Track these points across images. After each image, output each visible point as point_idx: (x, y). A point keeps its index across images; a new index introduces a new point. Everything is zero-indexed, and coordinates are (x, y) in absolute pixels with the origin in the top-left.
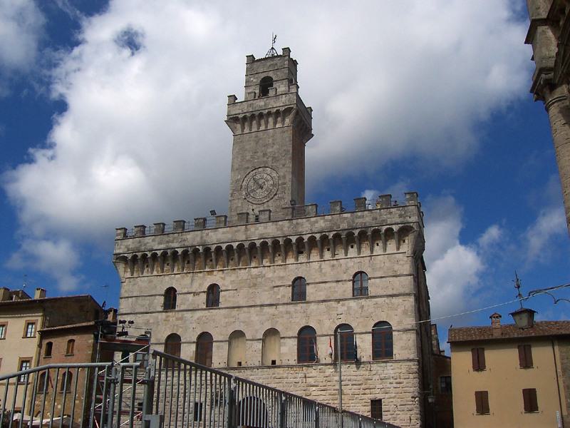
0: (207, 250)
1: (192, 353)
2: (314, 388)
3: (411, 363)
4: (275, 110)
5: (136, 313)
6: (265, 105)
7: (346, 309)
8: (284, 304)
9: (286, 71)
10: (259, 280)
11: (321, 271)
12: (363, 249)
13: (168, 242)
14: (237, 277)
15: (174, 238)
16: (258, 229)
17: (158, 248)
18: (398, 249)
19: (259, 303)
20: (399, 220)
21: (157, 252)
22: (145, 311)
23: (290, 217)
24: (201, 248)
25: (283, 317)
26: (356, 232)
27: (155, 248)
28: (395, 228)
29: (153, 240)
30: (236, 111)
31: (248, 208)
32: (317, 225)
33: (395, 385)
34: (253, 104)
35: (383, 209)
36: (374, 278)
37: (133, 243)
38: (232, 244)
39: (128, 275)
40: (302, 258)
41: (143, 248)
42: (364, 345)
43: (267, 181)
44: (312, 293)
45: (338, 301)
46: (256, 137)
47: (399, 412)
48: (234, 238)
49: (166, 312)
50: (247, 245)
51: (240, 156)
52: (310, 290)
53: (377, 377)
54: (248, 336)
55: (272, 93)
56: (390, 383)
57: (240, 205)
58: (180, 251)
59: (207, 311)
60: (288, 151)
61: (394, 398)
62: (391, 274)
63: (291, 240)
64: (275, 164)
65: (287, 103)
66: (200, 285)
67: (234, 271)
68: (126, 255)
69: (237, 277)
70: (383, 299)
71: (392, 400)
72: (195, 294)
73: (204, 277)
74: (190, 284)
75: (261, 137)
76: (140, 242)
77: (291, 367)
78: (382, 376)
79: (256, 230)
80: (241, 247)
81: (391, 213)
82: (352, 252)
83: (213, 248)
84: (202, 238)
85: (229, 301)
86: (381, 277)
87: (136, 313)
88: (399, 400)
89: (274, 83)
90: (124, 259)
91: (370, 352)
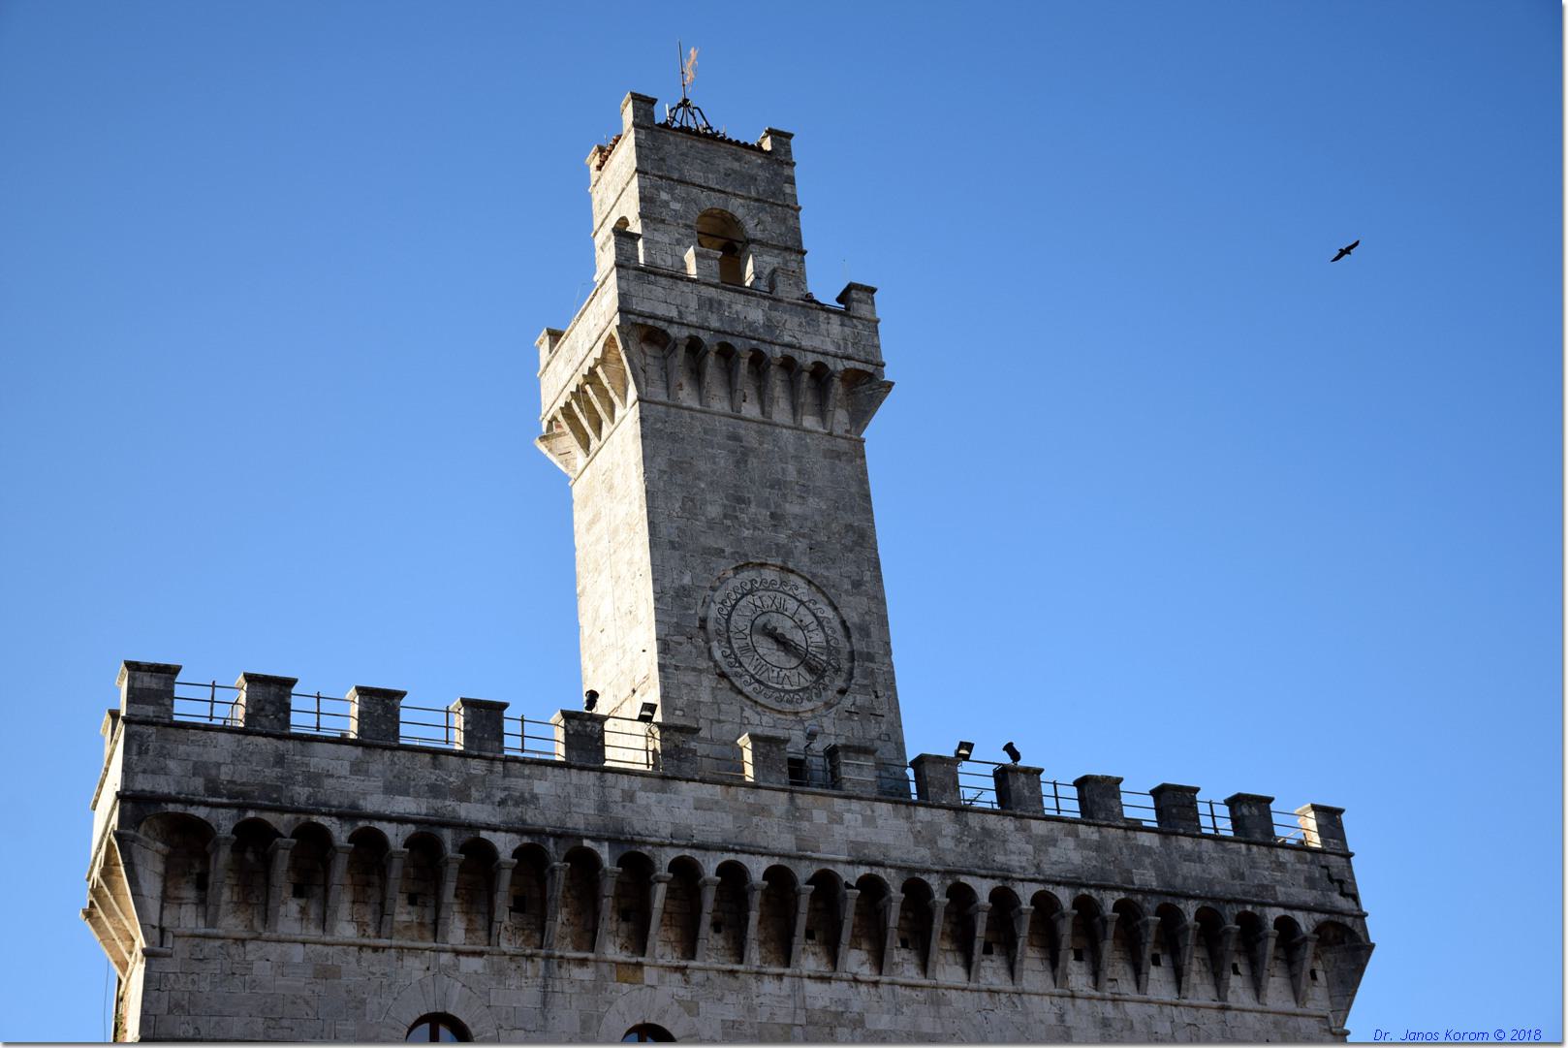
0: (636, 866)
6: (770, 326)
12: (1194, 978)
13: (435, 791)
14: (751, 1009)
15: (469, 780)
16: (836, 819)
17: (387, 810)
20: (1309, 897)
24: (604, 852)
26: (1190, 909)
30: (657, 302)
34: (720, 303)
38: (743, 859)
40: (992, 972)
41: (301, 793)
43: (801, 627)
48: (746, 838)
50: (804, 872)
57: (705, 696)
58: (505, 845)
64: (820, 570)
65: (850, 351)
67: (731, 980)
68: (201, 812)
73: (598, 987)
79: (831, 821)
80: (779, 877)
81: (1281, 866)
82: (1159, 980)
83: (665, 858)
84: (603, 807)
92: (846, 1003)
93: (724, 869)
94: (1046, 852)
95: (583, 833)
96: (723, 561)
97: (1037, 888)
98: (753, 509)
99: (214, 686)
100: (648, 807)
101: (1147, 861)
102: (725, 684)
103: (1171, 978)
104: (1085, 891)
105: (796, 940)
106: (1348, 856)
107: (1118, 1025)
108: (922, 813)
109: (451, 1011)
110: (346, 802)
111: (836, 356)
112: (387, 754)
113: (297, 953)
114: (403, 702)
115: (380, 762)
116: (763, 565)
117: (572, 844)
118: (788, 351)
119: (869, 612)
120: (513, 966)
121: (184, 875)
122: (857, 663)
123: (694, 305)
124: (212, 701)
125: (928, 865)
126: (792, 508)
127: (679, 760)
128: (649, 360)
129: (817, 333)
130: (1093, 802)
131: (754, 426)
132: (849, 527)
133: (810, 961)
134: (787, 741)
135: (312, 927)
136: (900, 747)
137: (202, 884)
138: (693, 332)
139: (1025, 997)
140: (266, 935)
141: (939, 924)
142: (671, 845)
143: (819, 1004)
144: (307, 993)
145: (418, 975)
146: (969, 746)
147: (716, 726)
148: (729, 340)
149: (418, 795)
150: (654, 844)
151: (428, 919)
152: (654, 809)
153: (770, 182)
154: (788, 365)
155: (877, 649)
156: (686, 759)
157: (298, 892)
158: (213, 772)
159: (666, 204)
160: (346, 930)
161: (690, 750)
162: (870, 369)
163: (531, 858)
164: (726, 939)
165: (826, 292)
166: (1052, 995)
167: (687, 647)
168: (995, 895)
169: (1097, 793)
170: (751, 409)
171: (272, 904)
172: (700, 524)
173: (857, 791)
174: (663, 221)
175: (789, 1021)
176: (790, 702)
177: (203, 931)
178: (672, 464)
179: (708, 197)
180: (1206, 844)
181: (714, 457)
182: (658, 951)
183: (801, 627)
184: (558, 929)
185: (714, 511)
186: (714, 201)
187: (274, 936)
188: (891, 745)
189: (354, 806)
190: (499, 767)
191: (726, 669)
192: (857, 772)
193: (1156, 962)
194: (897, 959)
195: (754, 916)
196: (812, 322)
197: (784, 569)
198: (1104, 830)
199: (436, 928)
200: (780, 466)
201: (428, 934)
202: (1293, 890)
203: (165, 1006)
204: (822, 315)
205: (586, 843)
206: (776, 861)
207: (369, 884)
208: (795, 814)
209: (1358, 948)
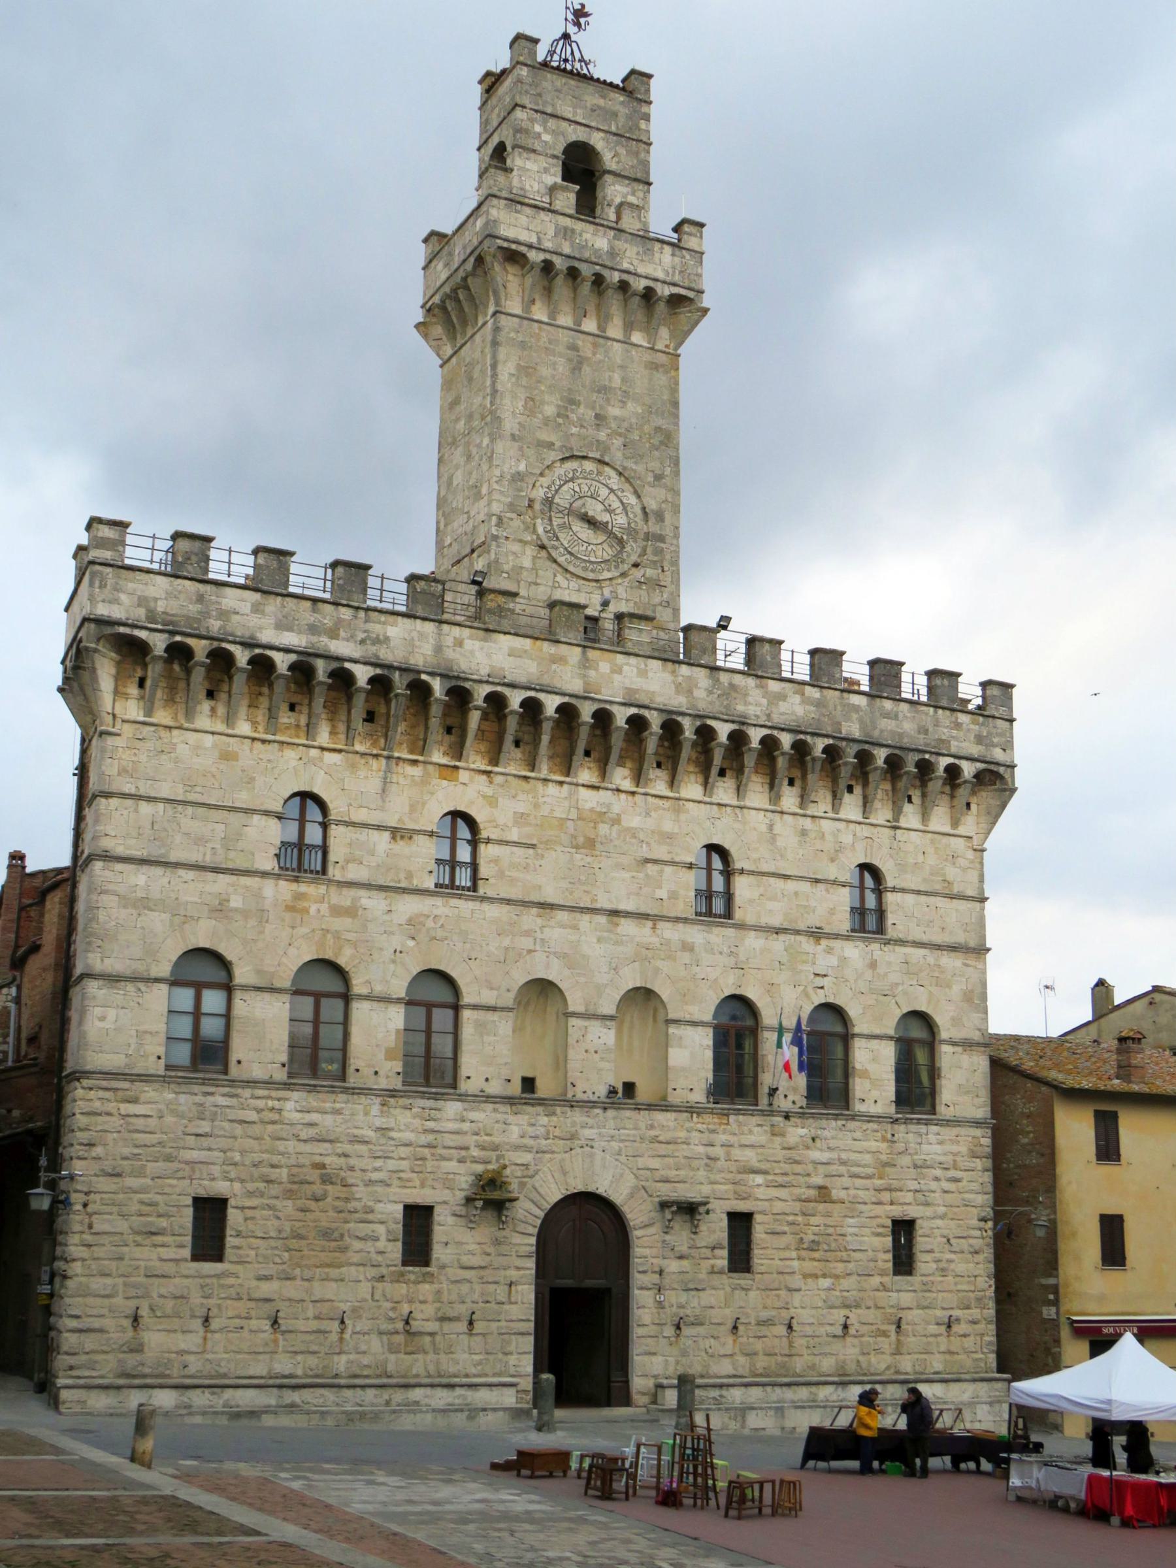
0: (459, 696)
1: (393, 1037)
2: (759, 1179)
3: (978, 1132)
5: (176, 865)
6: (612, 253)
7: (834, 961)
8: (677, 920)
10: (603, 829)
11: (773, 839)
12: (877, 804)
13: (313, 629)
14: (536, 806)
15: (339, 622)
16: (618, 670)
18: (955, 823)
19: (604, 903)
20: (975, 750)
22: (208, 860)
25: (675, 960)
26: (881, 755)
34: (573, 231)
35: (943, 708)
36: (903, 891)
37: (169, 595)
38: (541, 696)
39: (132, 709)
40: (724, 791)
42: (874, 1067)
43: (610, 511)
44: (751, 901)
45: (817, 934)
47: (953, 1256)
48: (546, 680)
49: (296, 880)
50: (586, 712)
51: (522, 395)
53: (905, 1160)
54: (575, 1003)
56: (937, 1179)
57: (527, 563)
59: (439, 901)
61: (942, 1217)
62: (938, 887)
64: (630, 464)
65: (677, 278)
66: (413, 808)
67: (523, 783)
68: (143, 634)
69: (536, 806)
70: (922, 952)
71: (939, 1222)
72: (397, 833)
73: (425, 781)
74: (386, 796)
75: (589, 354)
77: (691, 1110)
79: (613, 671)
80: (567, 712)
81: (958, 726)
82: (851, 806)
83: (481, 693)
85: (513, 881)
86: (919, 892)
87: (176, 865)
88: (952, 1223)
90: (131, 649)
91: (889, 1090)
92: (609, 806)
93: (525, 703)
94: (777, 705)
95: (421, 668)
96: (553, 453)
97: (766, 732)
98: (582, 410)
99: (154, 537)
100: (472, 652)
101: (855, 716)
102: (544, 553)
103: (861, 803)
104: (802, 737)
105: (575, 758)
106: (1011, 721)
107: (813, 835)
108: (684, 670)
109: (316, 791)
110: (247, 634)
111: (664, 282)
112: (279, 599)
113: (209, 740)
114: (293, 559)
115: (273, 605)
116: (584, 457)
117: (411, 677)
118: (625, 277)
119: (666, 501)
120: (363, 761)
121: (130, 677)
122: (651, 547)
123: (551, 233)
124: (153, 549)
125: (684, 709)
126: (614, 411)
127: (500, 616)
128: (510, 277)
129: (651, 261)
130: (820, 668)
131: (590, 338)
133: (586, 774)
134: (585, 607)
135: (219, 722)
136: (676, 612)
137: (141, 683)
138: (548, 256)
139: (745, 811)
140: (186, 725)
141: (686, 752)
142: (487, 682)
143: (588, 806)
144: (214, 769)
145: (294, 763)
146: (728, 619)
147: (533, 587)
148: (576, 264)
149: (300, 632)
150: (475, 681)
151: (303, 720)
152: (477, 654)
153: (629, 117)
154: (624, 286)
155: (668, 532)
156: (505, 617)
157: (210, 694)
158: (152, 604)
159: (539, 135)
160: (244, 728)
161: (509, 610)
162: (691, 294)
163: (381, 684)
164: (523, 753)
165: (661, 224)
166: (767, 811)
167: (517, 523)
168: (732, 736)
169: (825, 660)
170: (590, 325)
171: (191, 704)
172: (536, 421)
173: (636, 650)
174: (534, 151)
175: (564, 816)
176: (592, 571)
177: (141, 719)
178: (519, 367)
179: (575, 131)
180: (904, 707)
181: (555, 364)
182: (472, 758)
183: (610, 511)
184: (398, 737)
185: (550, 410)
186: (576, 134)
187: (191, 726)
188: (669, 611)
189: (252, 637)
190: (362, 614)
191: (546, 542)
193: (850, 789)
194: (651, 776)
195: (545, 739)
196: (649, 251)
197: (601, 462)
198: (826, 692)
199: (310, 730)
200: (607, 374)
201: (302, 734)
202: (964, 744)
203: (115, 771)
204: (657, 246)
205: (424, 677)
206: (566, 699)
207: (260, 694)
208: (585, 664)
209: (1005, 790)
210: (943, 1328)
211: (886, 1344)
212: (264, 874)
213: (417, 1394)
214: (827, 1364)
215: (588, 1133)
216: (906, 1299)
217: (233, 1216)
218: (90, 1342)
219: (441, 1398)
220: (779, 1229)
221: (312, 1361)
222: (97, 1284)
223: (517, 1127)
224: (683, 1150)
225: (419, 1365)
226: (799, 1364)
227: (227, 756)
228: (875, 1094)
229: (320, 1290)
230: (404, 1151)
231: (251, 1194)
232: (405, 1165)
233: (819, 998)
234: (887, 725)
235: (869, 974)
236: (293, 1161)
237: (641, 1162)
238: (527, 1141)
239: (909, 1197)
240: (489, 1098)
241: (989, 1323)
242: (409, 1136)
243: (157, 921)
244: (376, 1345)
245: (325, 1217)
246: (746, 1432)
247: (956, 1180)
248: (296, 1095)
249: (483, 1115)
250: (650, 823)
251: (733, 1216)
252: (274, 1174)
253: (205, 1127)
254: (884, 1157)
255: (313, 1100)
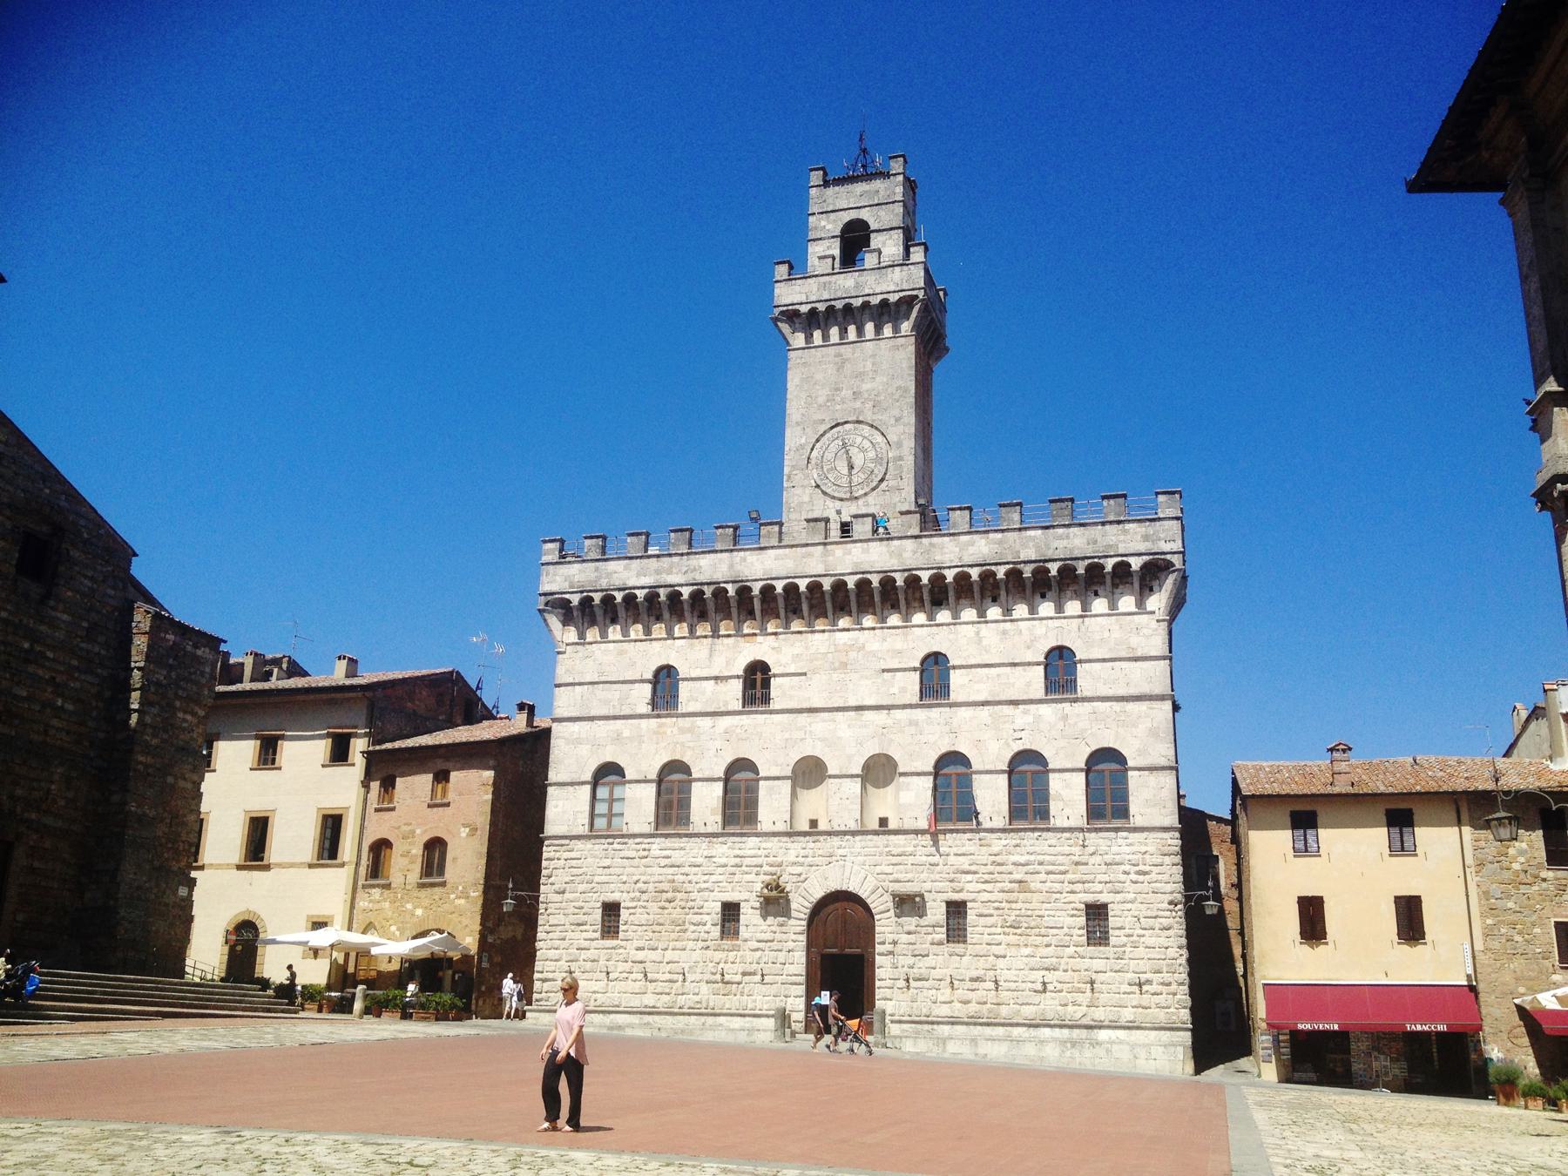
0: (744, 591)
2: (969, 877)
4: (880, 298)
5: (592, 719)
6: (857, 286)
7: (1031, 719)
8: (905, 707)
9: (899, 208)
10: (853, 655)
13: (658, 572)
20: (1142, 547)
21: (637, 592)
23: (916, 531)
26: (1054, 568)
27: (631, 583)
28: (1136, 563)
29: (626, 568)
31: (829, 509)
32: (971, 550)
33: (1134, 877)
35: (1111, 523)
39: (571, 634)
40: (944, 616)
41: (604, 584)
44: (962, 686)
46: (839, 355)
49: (658, 716)
51: (803, 395)
52: (956, 678)
53: (1097, 859)
55: (870, 260)
56: (1125, 873)
58: (686, 592)
60: (906, 391)
62: (1124, 654)
63: (918, 579)
70: (1108, 704)
71: (1129, 906)
74: (710, 658)
76: (597, 569)
78: (1108, 858)
83: (756, 588)
84: (731, 566)
86: (1104, 660)
89: (873, 236)
92: (856, 640)
132: (898, 388)
178: (802, 380)
185: (821, 400)
192: (862, 529)
208: (825, 554)
210: (1136, 989)
211: (1084, 998)
212: (641, 716)
213: (722, 1019)
214: (1028, 1011)
215: (841, 852)
216: (1098, 964)
217: (624, 914)
218: (546, 986)
219: (737, 1022)
220: (986, 912)
221: (665, 998)
222: (552, 954)
223: (793, 850)
224: (911, 860)
225: (731, 1003)
226: (1004, 1011)
227: (621, 653)
228: (1067, 811)
229: (669, 955)
230: (720, 870)
231: (633, 899)
232: (721, 878)
233: (1018, 747)
234: (1056, 544)
235: (1060, 725)
236: (656, 878)
237: (878, 869)
238: (800, 859)
239: (1099, 887)
240: (774, 834)
241: (1182, 984)
242: (723, 861)
243: (584, 750)
244: (704, 988)
245: (676, 914)
246: (946, 1055)
247: (1145, 873)
248: (658, 840)
249: (773, 843)
250: (886, 645)
251: (949, 904)
252: (643, 887)
253: (607, 862)
254: (1076, 858)
255: (668, 842)
